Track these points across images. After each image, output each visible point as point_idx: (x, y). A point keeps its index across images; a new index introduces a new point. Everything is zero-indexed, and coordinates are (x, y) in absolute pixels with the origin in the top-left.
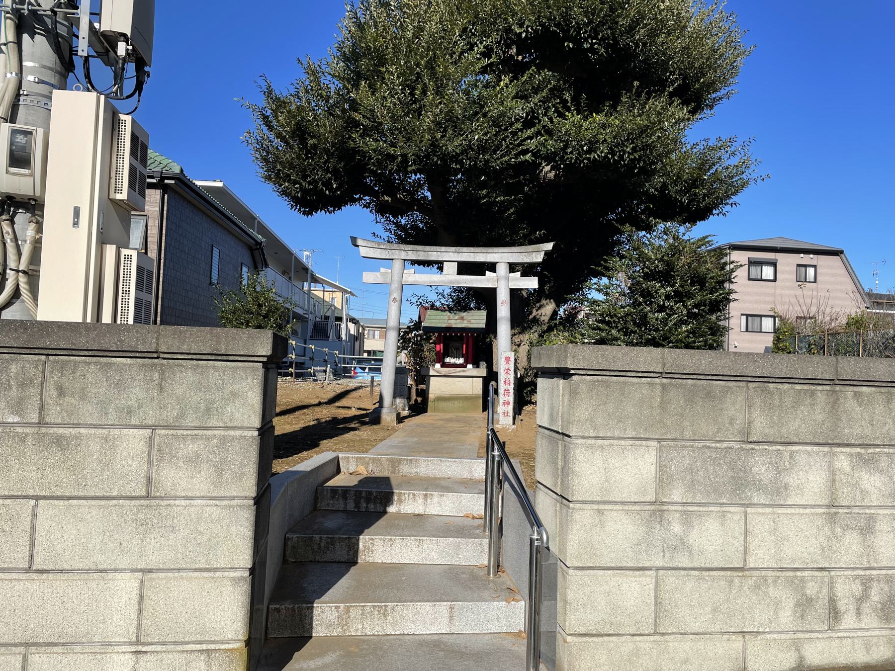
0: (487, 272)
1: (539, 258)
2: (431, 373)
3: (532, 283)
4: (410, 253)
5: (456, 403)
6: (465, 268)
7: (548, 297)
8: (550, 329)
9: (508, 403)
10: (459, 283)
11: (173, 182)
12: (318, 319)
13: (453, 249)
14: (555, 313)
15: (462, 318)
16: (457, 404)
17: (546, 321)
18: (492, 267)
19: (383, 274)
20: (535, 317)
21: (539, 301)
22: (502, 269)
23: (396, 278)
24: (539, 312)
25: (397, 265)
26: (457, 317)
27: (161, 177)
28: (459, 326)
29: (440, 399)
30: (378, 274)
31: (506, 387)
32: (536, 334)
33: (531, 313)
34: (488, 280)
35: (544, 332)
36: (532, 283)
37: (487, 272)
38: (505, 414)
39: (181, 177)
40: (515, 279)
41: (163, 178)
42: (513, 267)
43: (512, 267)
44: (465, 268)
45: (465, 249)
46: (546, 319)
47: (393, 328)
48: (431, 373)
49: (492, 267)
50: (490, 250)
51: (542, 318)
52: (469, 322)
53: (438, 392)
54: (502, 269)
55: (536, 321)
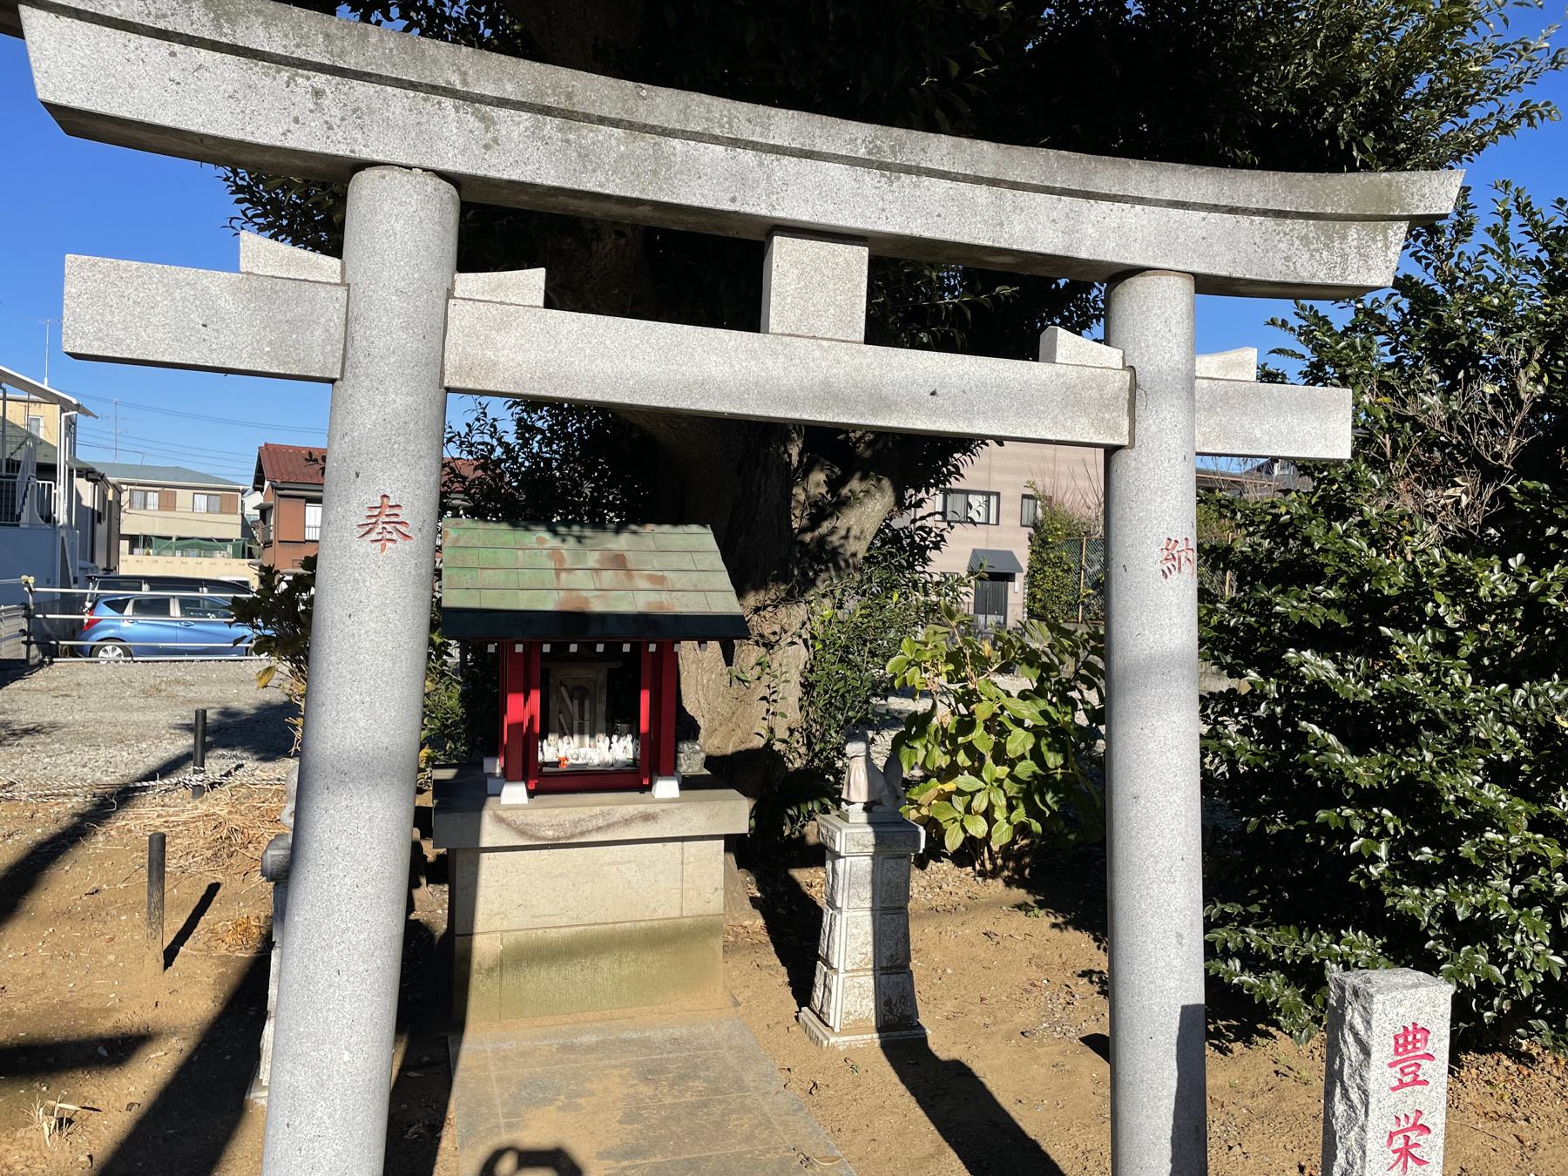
1: (1378, 261)
4: (515, 125)
5: (605, 963)
10: (880, 401)
13: (856, 136)
15: (619, 562)
16: (607, 969)
19: (268, 289)
23: (389, 334)
25: (398, 224)
26: (593, 559)
29: (530, 955)
30: (215, 282)
34: (1072, 398)
40: (1228, 398)
45: (940, 149)
47: (367, 770)
48: (486, 841)
50: (1107, 173)
52: (658, 581)
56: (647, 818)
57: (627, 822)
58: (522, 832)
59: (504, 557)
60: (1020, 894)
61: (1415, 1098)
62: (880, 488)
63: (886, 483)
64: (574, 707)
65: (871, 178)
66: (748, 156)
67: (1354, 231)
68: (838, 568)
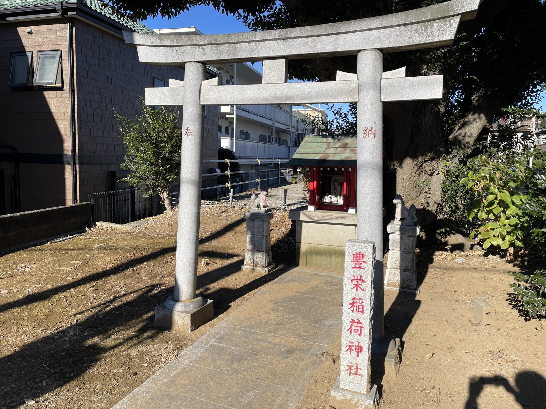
0: (339, 73)
1: (446, 32)
2: (301, 219)
3: (430, 87)
6: (301, 68)
7: (477, 110)
8: (475, 153)
9: (359, 349)
11: (74, 13)
12: (300, 132)
14: (484, 131)
17: (472, 143)
18: (348, 61)
20: (455, 138)
21: (462, 116)
22: (369, 63)
24: (463, 131)
27: (62, 9)
28: (338, 157)
31: (356, 316)
32: (456, 160)
33: (452, 131)
35: (469, 157)
36: (430, 87)
37: (339, 73)
38: (354, 369)
39: (81, 7)
41: (65, 11)
42: (391, 59)
43: (391, 59)
44: (301, 68)
45: (296, 31)
46: (471, 140)
48: (301, 219)
49: (348, 61)
50: (344, 26)
51: (468, 139)
53: (311, 241)
54: (369, 63)
55: (457, 142)
56: (342, 218)
57: (337, 218)
58: (309, 218)
59: (315, 145)
60: (517, 269)
61: (359, 272)
62: (480, 118)
63: (482, 115)
64: (338, 188)
65: (281, 42)
66: (253, 44)
67: (436, 24)
68: (460, 147)
